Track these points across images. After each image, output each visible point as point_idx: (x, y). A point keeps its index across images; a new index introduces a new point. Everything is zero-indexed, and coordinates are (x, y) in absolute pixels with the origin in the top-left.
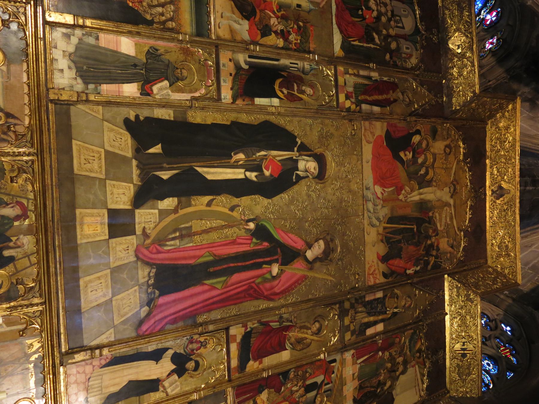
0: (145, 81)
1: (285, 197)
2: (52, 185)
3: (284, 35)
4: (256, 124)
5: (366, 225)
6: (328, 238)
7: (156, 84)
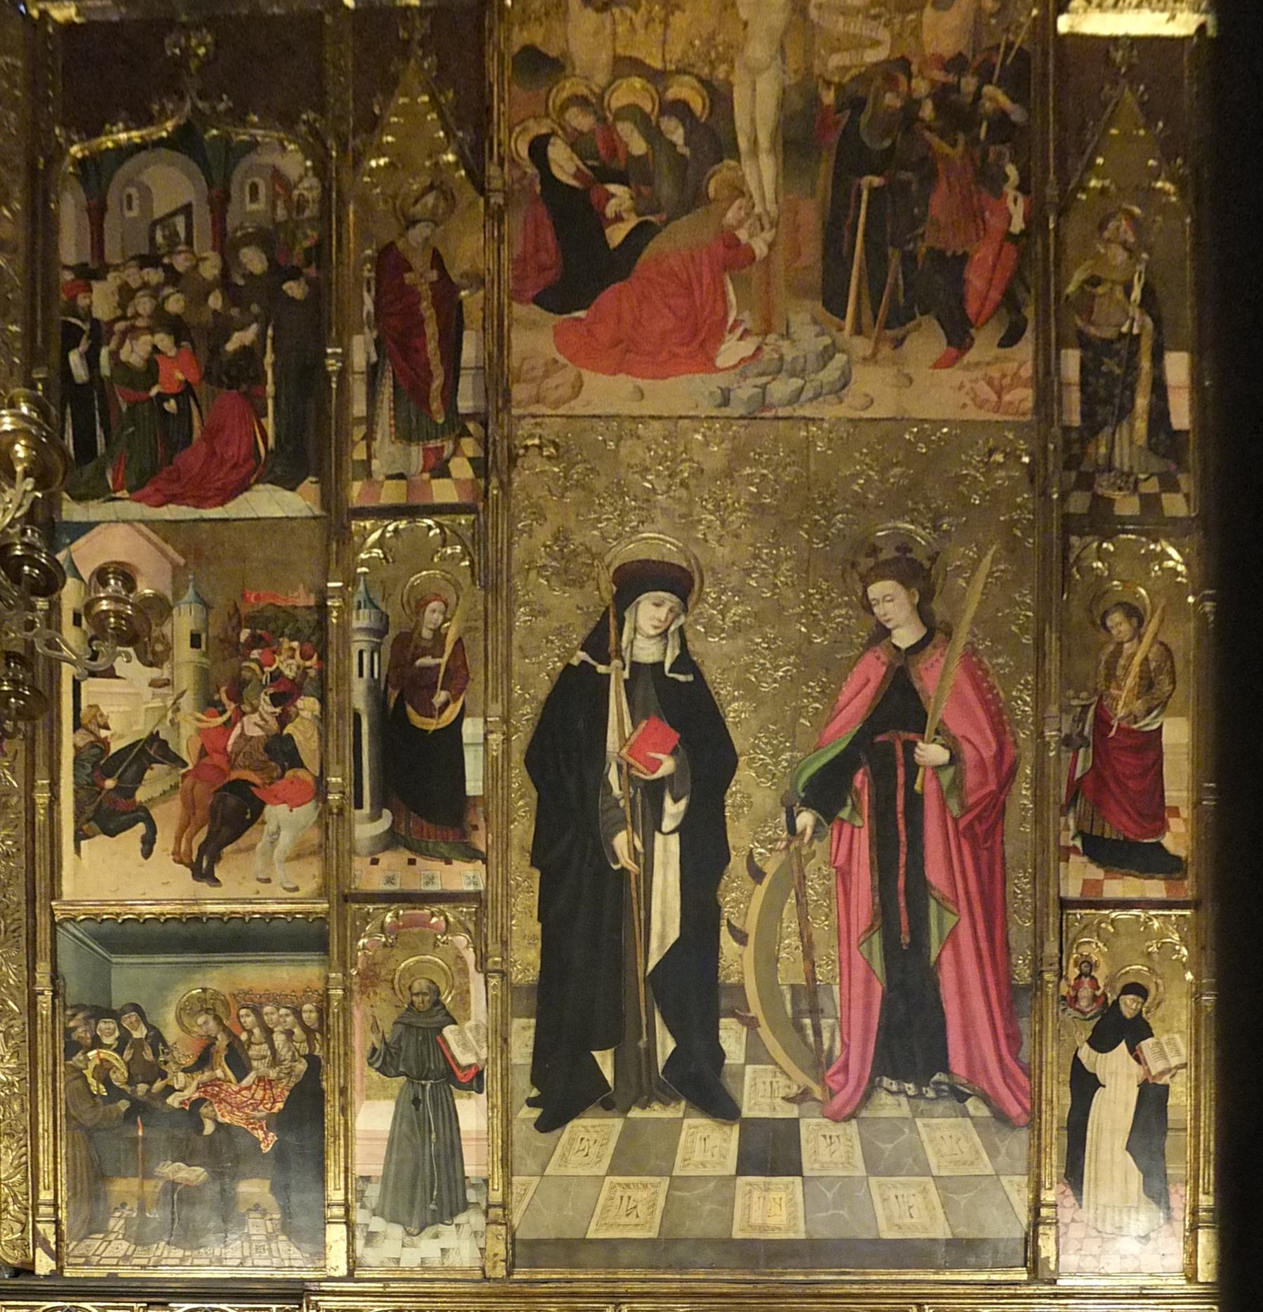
0: (449, 1082)
1: (736, 713)
2: (681, 1281)
3: (285, 695)
4: (535, 795)
5: (842, 411)
6: (866, 563)
7: (453, 1057)
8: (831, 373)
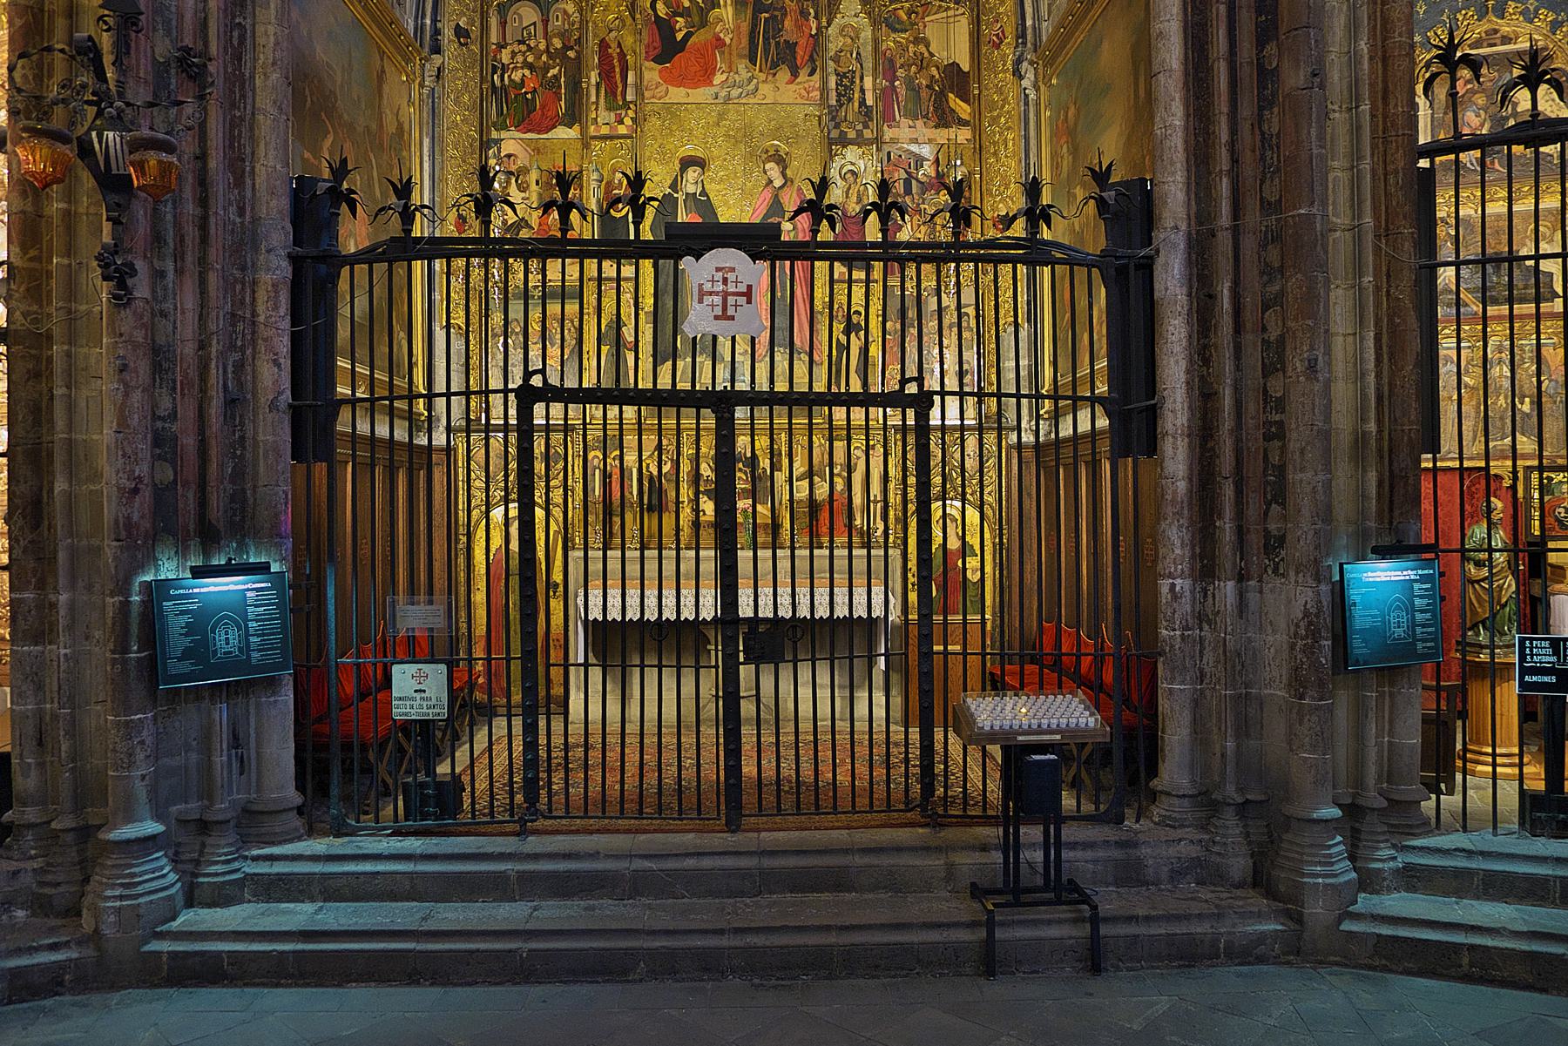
8: (751, 87)
